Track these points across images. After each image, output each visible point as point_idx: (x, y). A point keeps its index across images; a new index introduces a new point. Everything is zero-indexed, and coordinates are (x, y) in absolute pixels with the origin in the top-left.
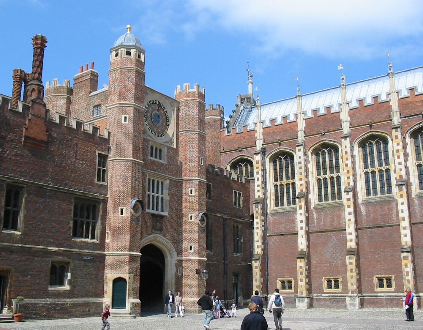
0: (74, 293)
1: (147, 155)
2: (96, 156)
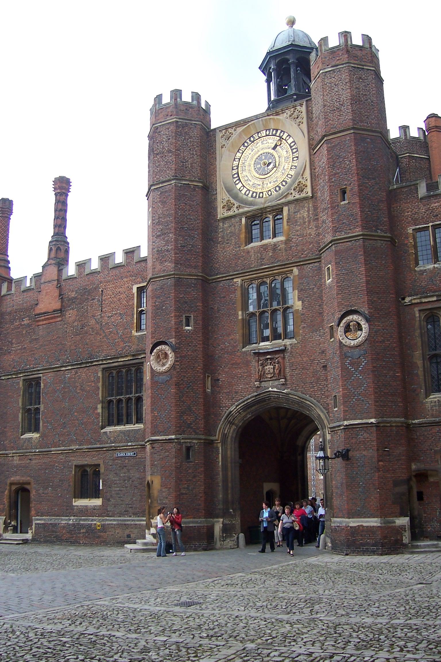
0: (107, 510)
2: (134, 294)
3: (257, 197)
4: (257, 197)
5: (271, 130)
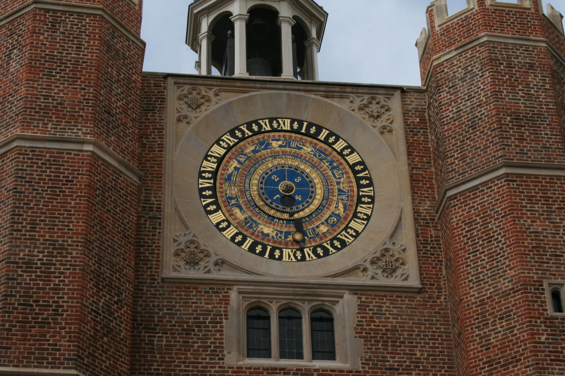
1: (218, 351)
3: (267, 256)
4: (267, 256)
5: (305, 124)
